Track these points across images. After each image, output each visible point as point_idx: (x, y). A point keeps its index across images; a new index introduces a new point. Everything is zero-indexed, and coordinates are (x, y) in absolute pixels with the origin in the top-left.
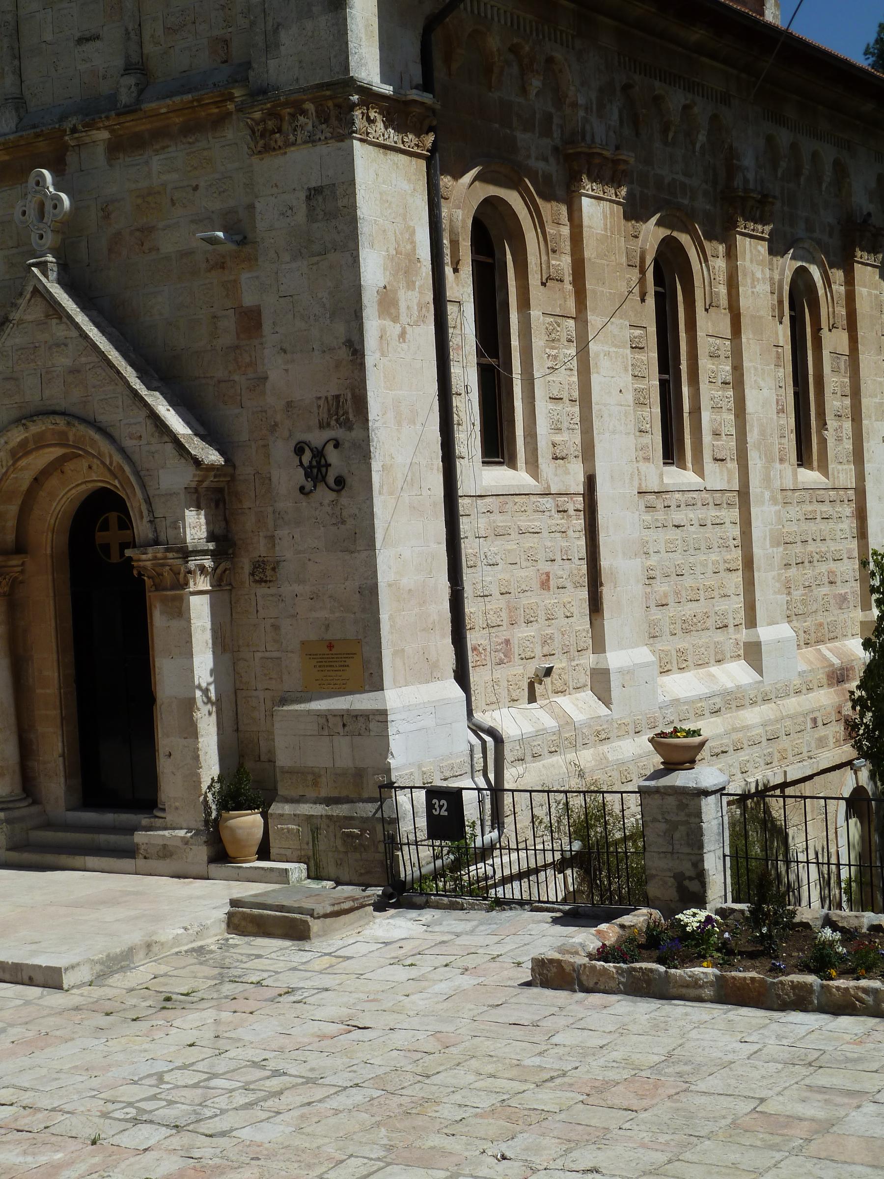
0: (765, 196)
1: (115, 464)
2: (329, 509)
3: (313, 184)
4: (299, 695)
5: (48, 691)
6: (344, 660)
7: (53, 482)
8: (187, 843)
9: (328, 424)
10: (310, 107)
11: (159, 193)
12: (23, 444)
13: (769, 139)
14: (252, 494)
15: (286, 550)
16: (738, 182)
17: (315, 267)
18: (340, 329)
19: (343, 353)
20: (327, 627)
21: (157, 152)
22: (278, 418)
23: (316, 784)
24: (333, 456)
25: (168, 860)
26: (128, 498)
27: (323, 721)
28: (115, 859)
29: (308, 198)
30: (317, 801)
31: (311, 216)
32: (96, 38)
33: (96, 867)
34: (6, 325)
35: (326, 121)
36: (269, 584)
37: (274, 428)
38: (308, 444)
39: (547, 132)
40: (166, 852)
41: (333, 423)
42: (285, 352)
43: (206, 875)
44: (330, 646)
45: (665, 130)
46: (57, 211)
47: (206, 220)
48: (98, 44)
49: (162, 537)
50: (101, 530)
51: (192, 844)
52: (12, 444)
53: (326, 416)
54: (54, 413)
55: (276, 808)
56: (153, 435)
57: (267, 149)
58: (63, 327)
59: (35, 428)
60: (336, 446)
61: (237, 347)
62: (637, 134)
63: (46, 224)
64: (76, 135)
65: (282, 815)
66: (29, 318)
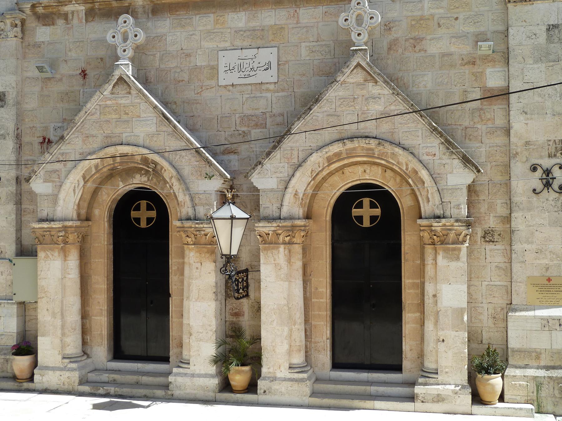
2: (553, 203)
3: (551, 23)
4: (525, 307)
5: (321, 300)
6: (559, 288)
7: (335, 178)
8: (456, 393)
9: (555, 156)
11: (429, 19)
14: (487, 192)
17: (550, 68)
20: (547, 269)
22: (519, 150)
23: (538, 357)
24: (556, 172)
25: (440, 404)
26: (418, 189)
27: (546, 322)
28: (398, 403)
29: (548, 30)
30: (538, 368)
31: (550, 39)
33: (383, 408)
34: (334, 83)
36: (495, 243)
40: (439, 399)
42: (526, 113)
43: (470, 412)
44: (549, 280)
46: (373, 21)
51: (460, 394)
52: (330, 154)
53: (553, 150)
54: (367, 137)
55: (509, 372)
56: (444, 154)
58: (378, 87)
59: (349, 145)
61: (481, 109)
66: (350, 80)
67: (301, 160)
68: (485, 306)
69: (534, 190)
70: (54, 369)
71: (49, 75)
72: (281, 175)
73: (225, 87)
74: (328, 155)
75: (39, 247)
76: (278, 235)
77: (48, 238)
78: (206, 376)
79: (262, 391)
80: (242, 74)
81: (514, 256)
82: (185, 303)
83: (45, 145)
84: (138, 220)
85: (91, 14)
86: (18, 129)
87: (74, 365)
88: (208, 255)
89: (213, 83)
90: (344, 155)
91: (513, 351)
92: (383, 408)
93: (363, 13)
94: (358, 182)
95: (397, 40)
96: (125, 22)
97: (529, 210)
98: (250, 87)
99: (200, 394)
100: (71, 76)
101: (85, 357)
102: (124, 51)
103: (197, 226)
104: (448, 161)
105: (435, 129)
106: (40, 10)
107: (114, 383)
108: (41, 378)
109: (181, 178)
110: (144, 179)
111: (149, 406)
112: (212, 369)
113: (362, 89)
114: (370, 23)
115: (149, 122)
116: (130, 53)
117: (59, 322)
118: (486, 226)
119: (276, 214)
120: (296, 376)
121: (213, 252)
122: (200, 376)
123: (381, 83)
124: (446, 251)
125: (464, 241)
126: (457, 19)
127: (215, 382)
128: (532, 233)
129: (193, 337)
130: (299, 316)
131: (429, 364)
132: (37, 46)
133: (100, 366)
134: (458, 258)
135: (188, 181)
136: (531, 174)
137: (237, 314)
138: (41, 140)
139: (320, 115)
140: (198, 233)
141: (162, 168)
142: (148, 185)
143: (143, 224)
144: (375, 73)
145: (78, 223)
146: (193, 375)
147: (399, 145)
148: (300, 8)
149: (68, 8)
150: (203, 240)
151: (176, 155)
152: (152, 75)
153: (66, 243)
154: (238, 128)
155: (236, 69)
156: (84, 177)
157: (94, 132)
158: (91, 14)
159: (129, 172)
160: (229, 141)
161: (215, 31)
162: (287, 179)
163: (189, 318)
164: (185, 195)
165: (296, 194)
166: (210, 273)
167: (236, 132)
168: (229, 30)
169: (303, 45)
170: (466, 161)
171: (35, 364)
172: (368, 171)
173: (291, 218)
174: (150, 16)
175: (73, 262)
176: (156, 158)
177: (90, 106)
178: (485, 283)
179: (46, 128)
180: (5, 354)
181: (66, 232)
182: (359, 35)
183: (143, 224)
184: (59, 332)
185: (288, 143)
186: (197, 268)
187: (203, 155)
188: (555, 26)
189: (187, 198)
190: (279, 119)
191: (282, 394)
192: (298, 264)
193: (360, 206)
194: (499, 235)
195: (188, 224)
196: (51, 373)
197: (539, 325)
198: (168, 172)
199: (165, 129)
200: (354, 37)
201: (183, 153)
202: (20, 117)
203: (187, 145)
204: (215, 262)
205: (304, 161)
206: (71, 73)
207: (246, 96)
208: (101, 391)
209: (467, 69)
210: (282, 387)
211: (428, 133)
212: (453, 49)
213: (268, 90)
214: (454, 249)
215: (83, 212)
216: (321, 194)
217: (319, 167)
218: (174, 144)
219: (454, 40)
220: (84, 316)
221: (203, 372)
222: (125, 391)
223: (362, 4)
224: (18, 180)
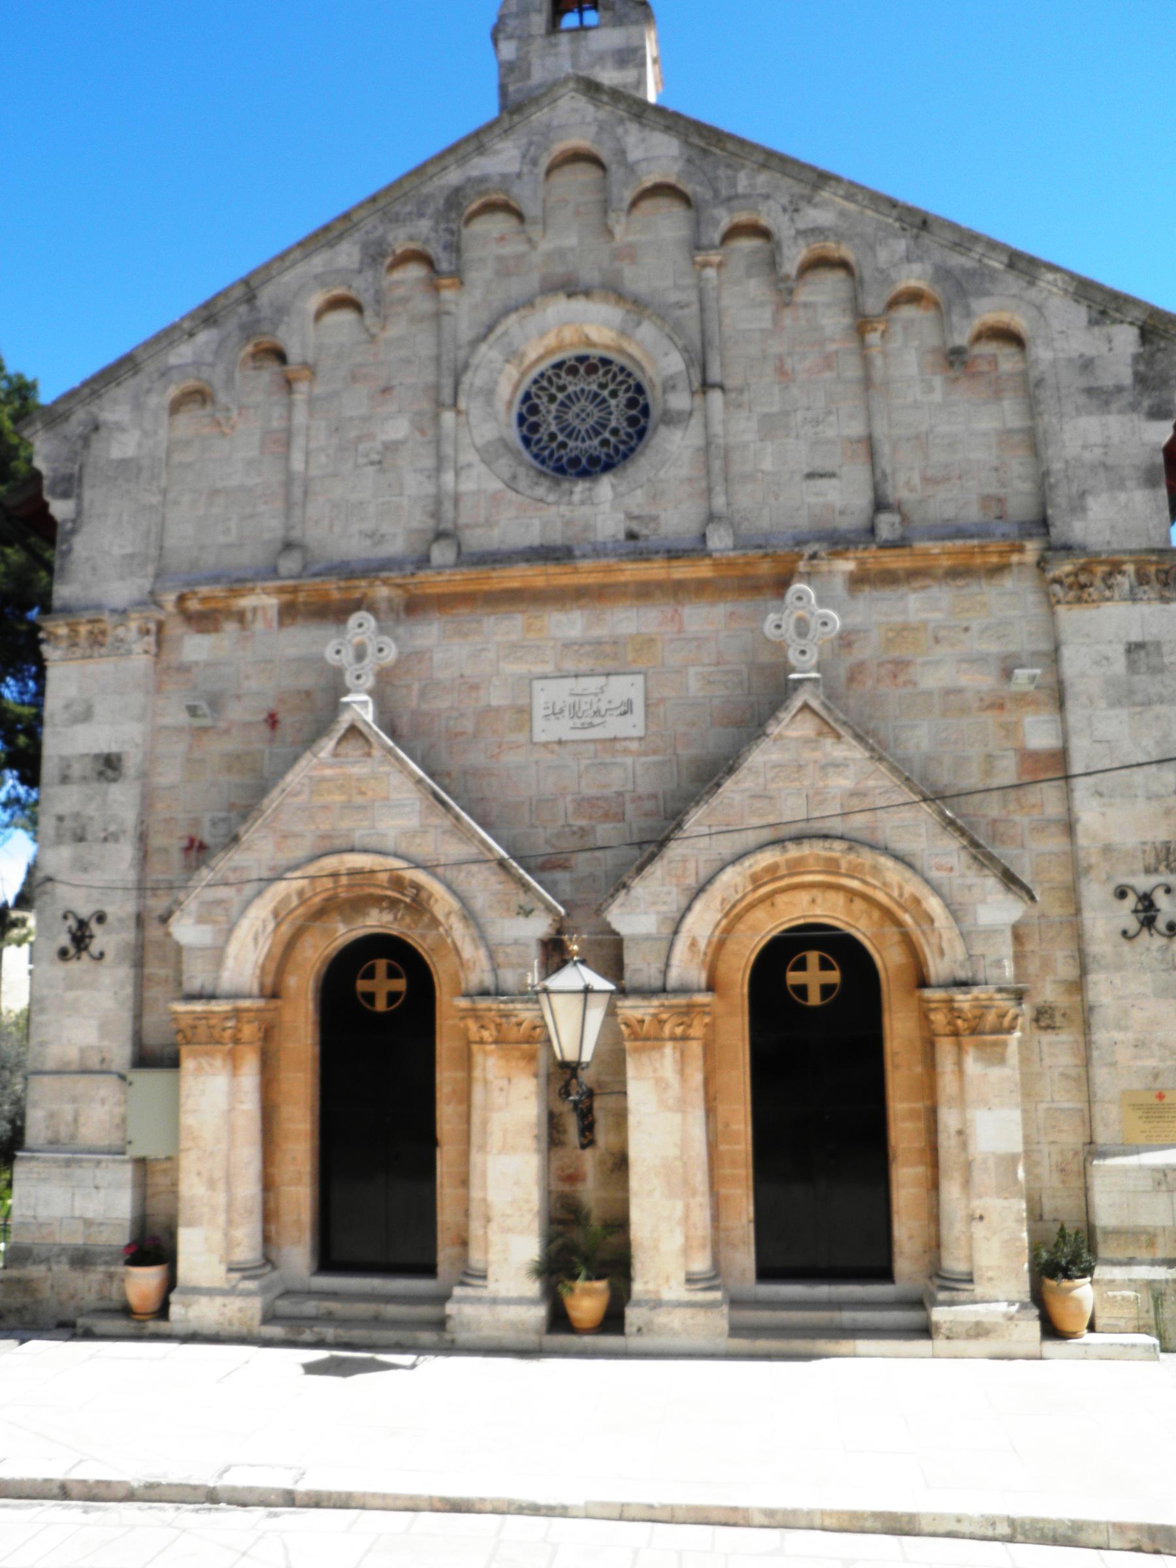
1: (906, 895)
5: (737, 1147)
7: (759, 914)
8: (1011, 1318)
10: (1130, 568)
11: (918, 629)
12: (772, 869)
14: (1037, 937)
17: (1137, 717)
20: (1156, 1076)
21: (915, 590)
22: (1093, 860)
23: (1151, 1244)
24: (1162, 901)
26: (924, 933)
27: (1160, 1176)
31: (1132, 667)
32: (832, 475)
35: (1148, 583)
36: (1057, 1031)
38: (1132, 888)
40: (979, 1331)
41: (1162, 868)
42: (1101, 795)
43: (1038, 1354)
46: (827, 629)
47: (979, 660)
50: (794, 969)
51: (1019, 1319)
55: (1101, 1272)
56: (969, 868)
57: (1079, 600)
60: (1168, 891)
63: (812, 640)
64: (815, 562)
65: (1112, 1281)
67: (702, 879)
68: (1046, 1149)
69: (1125, 933)
70: (210, 1292)
71: (207, 722)
72: (665, 908)
73: (545, 745)
74: (753, 870)
75: (184, 1050)
76: (662, 1022)
77: (202, 1032)
78: (520, 1301)
79: (634, 1329)
80: (578, 722)
81: (1095, 1054)
82: (476, 1158)
83: (193, 853)
84: (370, 997)
85: (289, 613)
86: (142, 822)
87: (251, 1285)
88: (522, 1064)
89: (521, 737)
90: (783, 871)
91: (1107, 1232)
92: (872, 1352)
93: (808, 616)
94: (801, 922)
95: (861, 664)
96: (360, 625)
97: (1119, 968)
98: (592, 747)
99: (509, 1338)
100: (248, 725)
101: (268, 1268)
102: (358, 677)
103: (502, 1006)
104: (977, 880)
105: (951, 823)
106: (193, 605)
107: (329, 1318)
108: (183, 1311)
109: (469, 916)
110: (387, 917)
111: (413, 1366)
112: (533, 1288)
113: (814, 750)
114: (823, 633)
115: (407, 809)
116: (369, 681)
117: (221, 1198)
118: (1039, 1000)
119: (657, 983)
120: (701, 1296)
121: (531, 1058)
122: (509, 1301)
123: (847, 737)
124: (980, 1046)
125: (1010, 1030)
126: (966, 629)
127: (540, 1312)
128: (1126, 1012)
129: (494, 1226)
130: (700, 1178)
131: (954, 1263)
132: (184, 669)
133: (297, 1286)
134: (1002, 1060)
135: (482, 921)
136: (1116, 903)
137: (573, 1178)
138: (185, 843)
139: (738, 798)
140: (504, 1020)
141: (430, 896)
142: (394, 930)
143: (381, 1005)
144: (837, 720)
145: (260, 1003)
146: (494, 1301)
147: (886, 851)
148: (683, 605)
149: (246, 602)
150: (514, 1034)
151: (460, 871)
152: (404, 724)
153: (236, 1041)
154: (572, 821)
155: (566, 713)
156: (275, 914)
157: (297, 828)
158: (289, 613)
159: (357, 905)
160: (553, 846)
161: (525, 643)
162: (677, 916)
163: (484, 1188)
164: (477, 948)
165: (693, 944)
166: (526, 1098)
167: (567, 829)
168: (551, 644)
169: (692, 671)
170: (1010, 879)
171: (171, 1283)
172: (819, 900)
173: (684, 990)
174: (402, 615)
175: (249, 1079)
176: (421, 877)
177: (294, 778)
178: (1043, 1106)
179: (196, 822)
180: (107, 1263)
181: (239, 1020)
182: (803, 652)
183: (381, 1005)
184: (221, 1219)
185: (675, 850)
186: (501, 1089)
187: (513, 871)
189: (482, 954)
190: (649, 805)
191: (674, 1333)
192: (697, 1078)
193: (801, 966)
194: (1064, 1015)
195: (483, 1003)
196: (204, 1300)
197: (1150, 1182)
198: (443, 902)
199: (435, 821)
200: (793, 657)
201: (474, 868)
202: (147, 802)
203: (481, 853)
204: (536, 1076)
205: (710, 881)
206: (248, 718)
207: (585, 762)
208: (308, 1336)
209: (990, 717)
210: (674, 1320)
211: (938, 830)
212: (964, 681)
213: (626, 751)
214: (995, 1044)
215: (269, 980)
216: (731, 946)
217: (737, 892)
218: (454, 849)
219: (964, 666)
220: (268, 1184)
221: (514, 1294)
222: (358, 1334)
223: (805, 599)
224: (140, 920)
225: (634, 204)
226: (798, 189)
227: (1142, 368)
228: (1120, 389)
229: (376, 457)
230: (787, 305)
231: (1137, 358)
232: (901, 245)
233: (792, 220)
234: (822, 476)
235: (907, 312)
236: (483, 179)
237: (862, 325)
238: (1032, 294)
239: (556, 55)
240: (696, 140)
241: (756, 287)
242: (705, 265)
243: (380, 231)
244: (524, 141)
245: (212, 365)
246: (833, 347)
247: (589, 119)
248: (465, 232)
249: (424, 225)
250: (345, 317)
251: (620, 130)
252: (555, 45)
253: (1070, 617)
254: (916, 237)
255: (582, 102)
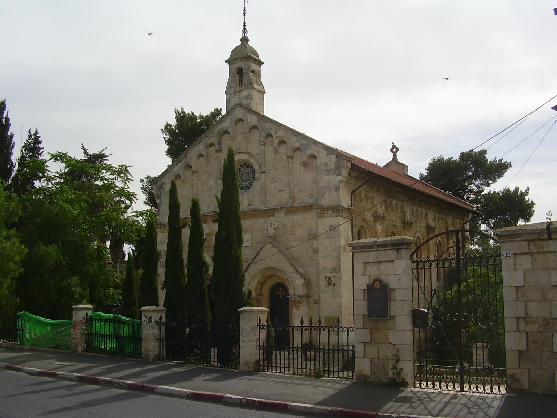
0: (412, 222)
1: (286, 278)
3: (331, 225)
13: (412, 209)
15: (322, 297)
16: (406, 219)
18: (335, 253)
19: (336, 258)
20: (330, 313)
24: (333, 279)
32: (283, 191)
37: (321, 272)
39: (371, 212)
41: (333, 272)
45: (392, 209)
48: (283, 192)
49: (296, 294)
57: (322, 217)
60: (334, 277)
62: (387, 210)
69: (326, 285)
126: (304, 223)
188: (332, 226)
213: (248, 249)
225: (250, 131)
226: (277, 127)
227: (336, 164)
228: (332, 169)
229: (208, 189)
230: (276, 153)
231: (336, 162)
232: (295, 139)
233: (276, 134)
234: (281, 191)
235: (298, 153)
236: (223, 128)
237: (288, 157)
238: (317, 149)
239: (235, 98)
240: (259, 117)
241: (271, 148)
242: (261, 145)
243: (206, 141)
244: (230, 118)
245: (180, 171)
246: (284, 162)
247: (241, 113)
248: (222, 138)
249: (214, 138)
250: (201, 159)
251: (247, 115)
252: (236, 95)
253: (321, 221)
254: (297, 137)
255: (240, 109)
